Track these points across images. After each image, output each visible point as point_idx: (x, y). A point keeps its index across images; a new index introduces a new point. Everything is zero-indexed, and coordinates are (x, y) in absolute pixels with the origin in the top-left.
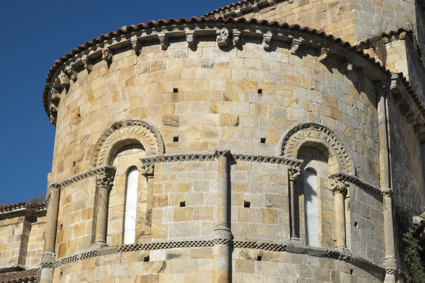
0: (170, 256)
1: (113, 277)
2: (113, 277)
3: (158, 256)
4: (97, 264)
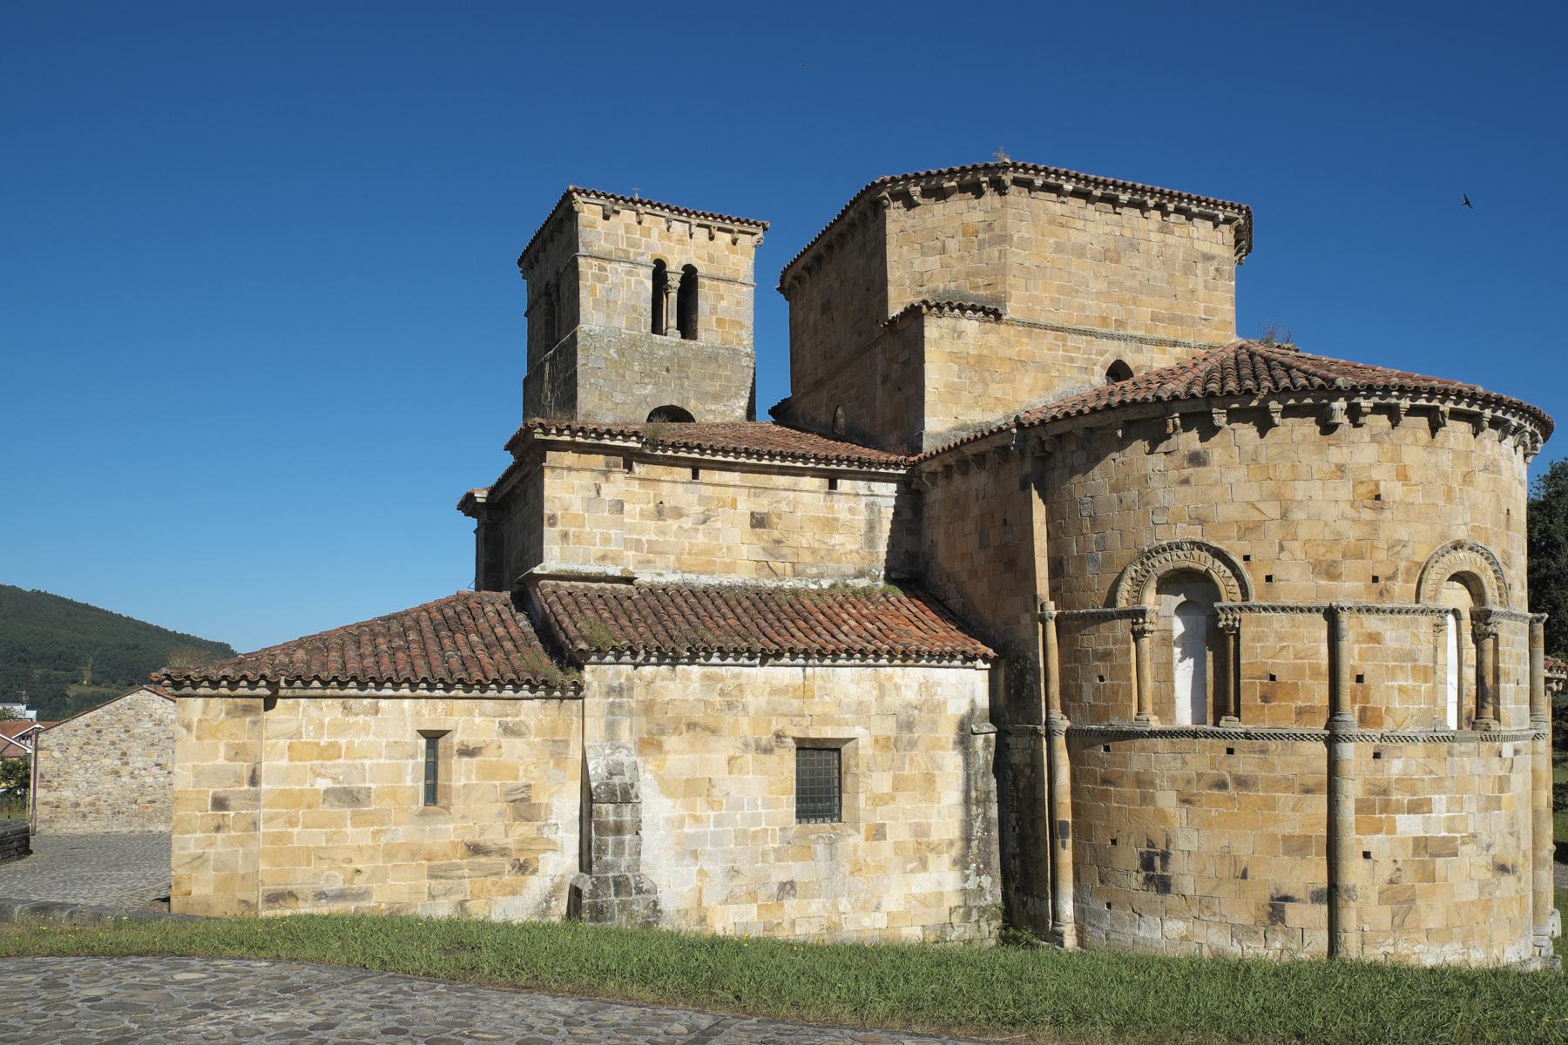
0: (1516, 752)
1: (1472, 775)
2: (1472, 775)
3: (1507, 749)
4: (1450, 754)
